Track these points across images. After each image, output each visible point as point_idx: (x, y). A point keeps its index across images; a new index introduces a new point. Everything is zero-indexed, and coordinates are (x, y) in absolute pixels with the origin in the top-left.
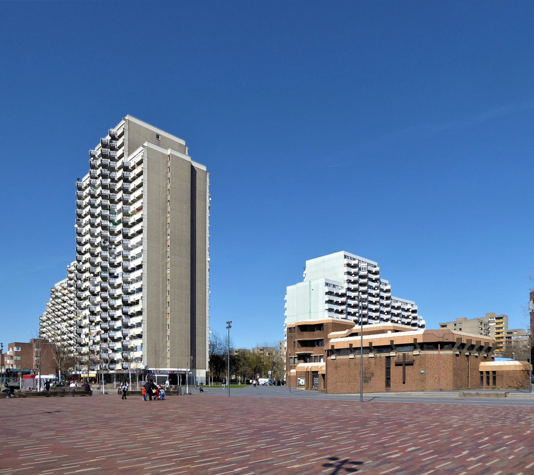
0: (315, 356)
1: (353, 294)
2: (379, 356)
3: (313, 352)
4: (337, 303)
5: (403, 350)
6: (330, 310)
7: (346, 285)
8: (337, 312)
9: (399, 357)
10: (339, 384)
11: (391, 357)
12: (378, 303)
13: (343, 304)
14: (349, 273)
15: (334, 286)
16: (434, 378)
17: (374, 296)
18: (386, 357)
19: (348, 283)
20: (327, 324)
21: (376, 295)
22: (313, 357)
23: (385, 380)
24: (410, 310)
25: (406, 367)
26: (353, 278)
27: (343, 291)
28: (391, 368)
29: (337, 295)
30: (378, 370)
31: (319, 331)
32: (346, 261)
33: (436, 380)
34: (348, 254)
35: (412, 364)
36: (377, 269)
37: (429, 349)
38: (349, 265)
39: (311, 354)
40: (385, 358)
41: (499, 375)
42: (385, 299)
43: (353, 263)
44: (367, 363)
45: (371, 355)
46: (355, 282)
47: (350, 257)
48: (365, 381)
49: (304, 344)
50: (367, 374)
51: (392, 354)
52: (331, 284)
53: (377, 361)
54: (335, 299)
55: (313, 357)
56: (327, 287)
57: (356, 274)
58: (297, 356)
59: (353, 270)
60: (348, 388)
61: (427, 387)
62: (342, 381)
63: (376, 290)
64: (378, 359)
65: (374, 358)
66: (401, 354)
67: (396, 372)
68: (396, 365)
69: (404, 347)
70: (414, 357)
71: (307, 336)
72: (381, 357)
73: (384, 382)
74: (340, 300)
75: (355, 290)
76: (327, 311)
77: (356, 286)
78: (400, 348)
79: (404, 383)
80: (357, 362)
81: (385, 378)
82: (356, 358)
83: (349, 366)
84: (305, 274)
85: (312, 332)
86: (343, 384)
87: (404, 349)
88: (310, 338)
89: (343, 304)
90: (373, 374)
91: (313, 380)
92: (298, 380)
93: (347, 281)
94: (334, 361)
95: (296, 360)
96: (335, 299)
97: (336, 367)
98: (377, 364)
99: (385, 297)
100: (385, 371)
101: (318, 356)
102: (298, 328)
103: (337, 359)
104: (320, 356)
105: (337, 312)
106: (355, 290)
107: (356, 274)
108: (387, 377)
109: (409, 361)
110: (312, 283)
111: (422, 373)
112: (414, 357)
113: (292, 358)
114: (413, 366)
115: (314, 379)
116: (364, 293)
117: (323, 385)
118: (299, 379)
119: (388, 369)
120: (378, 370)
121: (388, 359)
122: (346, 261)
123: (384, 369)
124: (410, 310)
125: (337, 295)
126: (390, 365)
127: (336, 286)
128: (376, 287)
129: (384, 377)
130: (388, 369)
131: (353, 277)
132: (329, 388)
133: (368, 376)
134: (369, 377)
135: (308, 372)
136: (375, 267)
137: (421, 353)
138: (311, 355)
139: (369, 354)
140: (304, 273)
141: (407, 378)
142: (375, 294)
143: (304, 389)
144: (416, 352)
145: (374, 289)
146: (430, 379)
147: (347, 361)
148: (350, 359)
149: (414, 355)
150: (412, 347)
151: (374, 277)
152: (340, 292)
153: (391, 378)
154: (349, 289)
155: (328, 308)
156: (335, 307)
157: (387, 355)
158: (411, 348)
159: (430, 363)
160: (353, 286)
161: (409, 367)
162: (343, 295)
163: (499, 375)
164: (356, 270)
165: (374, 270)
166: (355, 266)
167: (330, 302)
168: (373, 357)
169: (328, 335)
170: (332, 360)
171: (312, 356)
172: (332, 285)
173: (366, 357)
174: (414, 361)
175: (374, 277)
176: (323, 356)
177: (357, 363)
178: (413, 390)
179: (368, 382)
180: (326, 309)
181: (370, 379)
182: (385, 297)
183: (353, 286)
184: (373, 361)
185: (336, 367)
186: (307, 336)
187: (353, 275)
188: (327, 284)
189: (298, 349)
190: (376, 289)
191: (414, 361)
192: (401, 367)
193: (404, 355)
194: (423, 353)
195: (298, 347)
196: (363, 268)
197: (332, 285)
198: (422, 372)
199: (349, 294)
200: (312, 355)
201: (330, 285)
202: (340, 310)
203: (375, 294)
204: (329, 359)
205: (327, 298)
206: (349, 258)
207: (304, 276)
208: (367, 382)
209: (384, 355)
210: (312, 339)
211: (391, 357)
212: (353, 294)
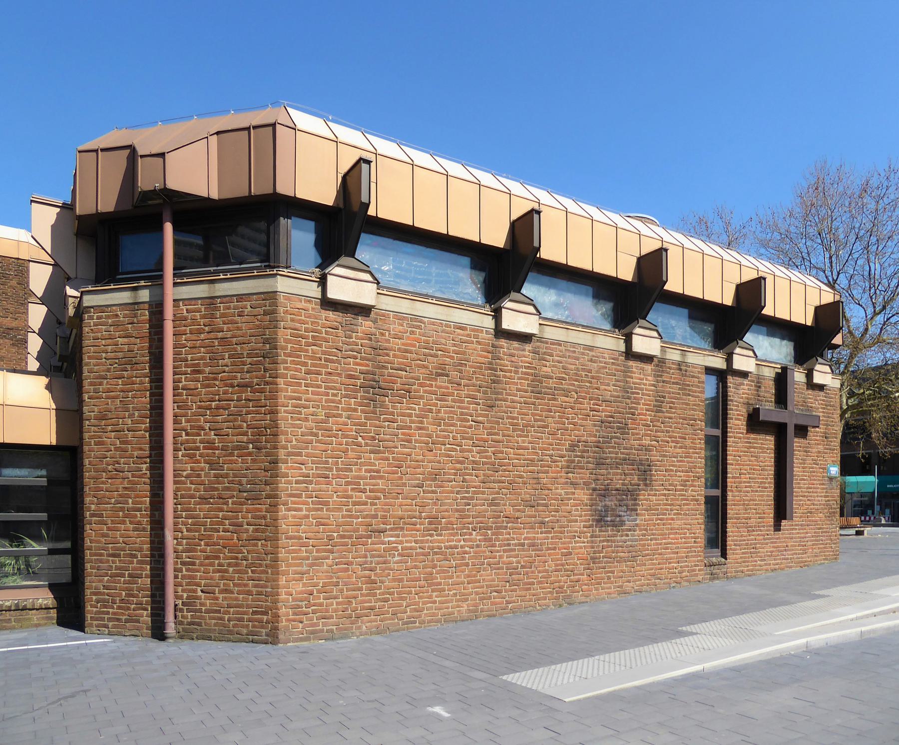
10: (407, 539)
30: (670, 449)
44: (610, 390)
60: (488, 575)
62: (434, 520)
64: (673, 375)
65: (649, 368)
82: (541, 339)
86: (441, 540)
90: (645, 472)
94: (350, 329)
98: (666, 407)
103: (385, 315)
132: (298, 588)
147: (477, 355)
170: (331, 315)
177: (551, 383)
204: (290, 296)
208: (614, 525)
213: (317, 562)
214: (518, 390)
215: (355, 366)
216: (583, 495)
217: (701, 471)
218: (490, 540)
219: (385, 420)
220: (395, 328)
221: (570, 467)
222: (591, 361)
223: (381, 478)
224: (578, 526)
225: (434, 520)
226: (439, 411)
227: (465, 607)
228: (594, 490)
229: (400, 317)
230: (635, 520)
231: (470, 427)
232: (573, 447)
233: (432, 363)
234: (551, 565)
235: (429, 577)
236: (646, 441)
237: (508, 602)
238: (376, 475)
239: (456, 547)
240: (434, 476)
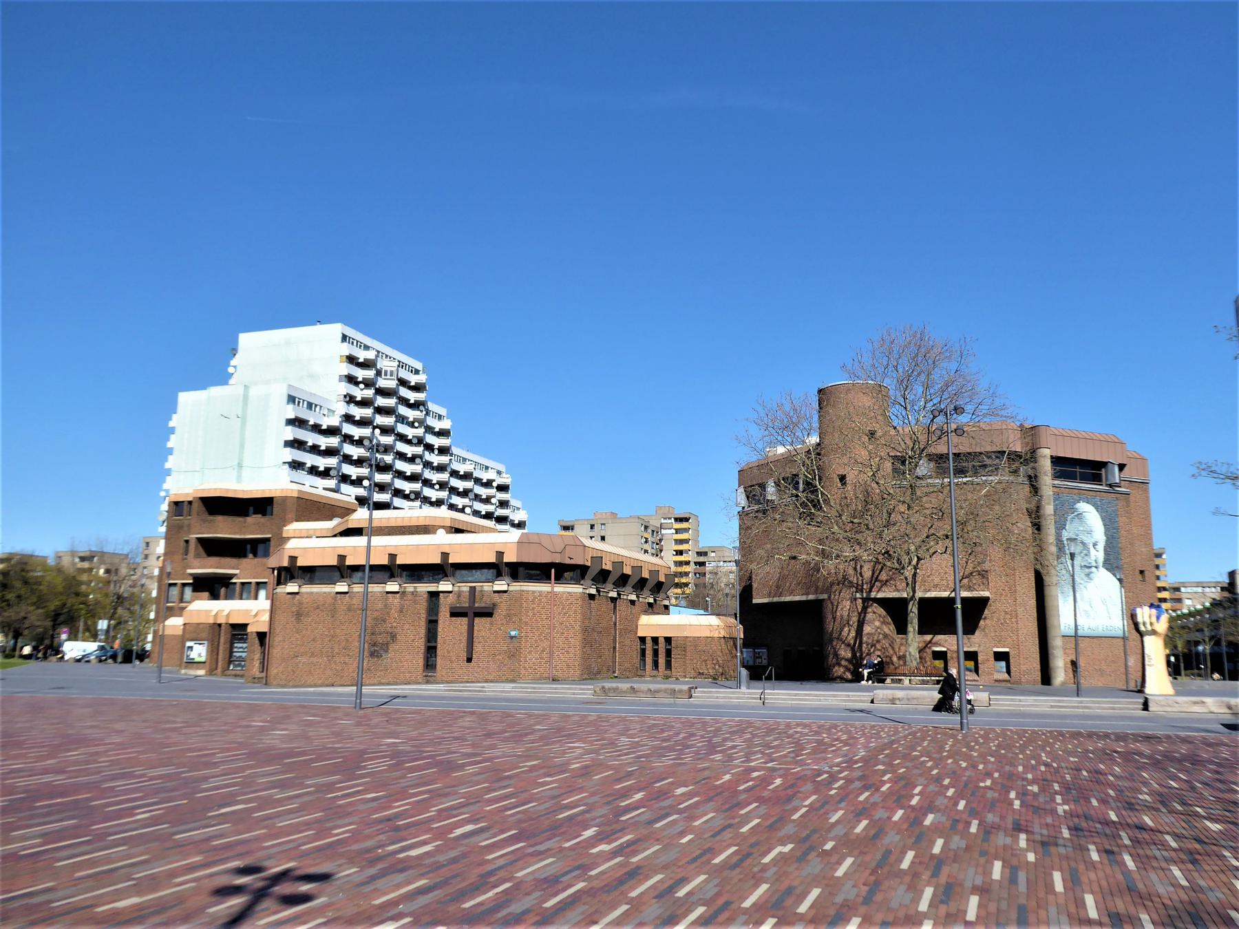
0: (243, 584)
1: (357, 432)
2: (411, 589)
3: (237, 572)
4: (315, 449)
5: (470, 579)
6: (296, 465)
7: (342, 408)
8: (313, 471)
9: (459, 594)
10: (303, 659)
11: (441, 594)
12: (418, 460)
13: (330, 452)
14: (351, 379)
15: (310, 405)
16: (540, 649)
17: (409, 442)
18: (429, 592)
19: (348, 403)
20: (285, 499)
21: (415, 441)
22: (238, 587)
23: (422, 651)
24: (495, 484)
25: (477, 620)
26: (360, 393)
27: (334, 421)
28: (440, 622)
29: (317, 428)
31: (260, 516)
32: (346, 349)
33: (544, 655)
34: (350, 332)
35: (490, 615)
36: (421, 378)
37: (531, 578)
38: (351, 360)
39: (231, 576)
40: (426, 596)
42: (436, 452)
43: (362, 355)
44: (380, 606)
45: (393, 586)
46: (364, 403)
47: (357, 341)
48: (372, 655)
49: (213, 548)
50: (380, 634)
51: (445, 586)
52: (304, 401)
53: (407, 602)
54: (312, 438)
55: (238, 587)
56: (291, 406)
57: (368, 384)
58: (191, 581)
59: (361, 374)
60: (328, 672)
61: (523, 672)
62: (313, 653)
63: (417, 428)
64: (410, 597)
65: (398, 595)
66: (465, 588)
67: (451, 631)
68: (454, 614)
69: (474, 571)
71: (225, 529)
73: (422, 656)
74: (324, 442)
75: (363, 423)
76: (287, 466)
77: (367, 412)
78: (464, 572)
79: (469, 660)
80: (354, 602)
81: (423, 647)
82: (353, 592)
83: (333, 611)
84: (235, 367)
85: (241, 519)
86: (314, 660)
87: (472, 576)
88: (234, 534)
89: (330, 452)
90: (393, 637)
91: (232, 647)
92: (189, 647)
93: (345, 396)
94: (294, 598)
95: (188, 591)
96: (312, 438)
97: (299, 615)
99: (436, 447)
100: (424, 628)
101: (250, 583)
102: (201, 504)
103: (303, 593)
104: (258, 583)
105: (313, 471)
106: (363, 423)
107: (368, 384)
109: (483, 605)
110: (253, 392)
111: (512, 637)
112: (496, 597)
113: (175, 584)
114: (493, 619)
115: (236, 645)
116: (385, 431)
117: (258, 662)
118: (189, 644)
119: (432, 624)
120: (406, 627)
121: (434, 599)
122: (346, 349)
123: (423, 623)
124: (495, 484)
125: (317, 428)
126: (437, 615)
127: (316, 405)
128: (415, 420)
129: (420, 644)
130: (432, 624)
131: (362, 390)
132: (276, 671)
133: (380, 639)
134: (382, 644)
135: (220, 625)
136: (417, 372)
137: (511, 588)
138: (231, 578)
139: (385, 584)
140: (233, 362)
141: (478, 647)
142: (413, 437)
143: (201, 672)
144: (500, 585)
145: (411, 425)
146: (530, 652)
147: (330, 600)
148: (338, 595)
149: (495, 592)
150: (491, 570)
151: (412, 396)
152: (325, 423)
153: (439, 646)
154: (348, 418)
155: (290, 460)
156: (310, 460)
157: (432, 587)
158: (490, 573)
159: (530, 613)
160: (358, 413)
161: (484, 620)
162: (332, 431)
164: (370, 374)
165: (413, 379)
166: (366, 365)
167: (297, 444)
168: (397, 593)
169: (285, 528)
171: (235, 583)
172: (305, 403)
174: (494, 605)
175: (412, 396)
176: (266, 583)
177: (355, 607)
178: (491, 677)
180: (285, 463)
181: (385, 647)
182: (436, 447)
183: (358, 413)
184: (396, 600)
185: (299, 615)
186: (225, 529)
187: (362, 386)
188: (291, 399)
189: (196, 562)
190: (416, 424)
191: (494, 605)
192: (465, 620)
193: (473, 589)
194: (517, 587)
195: (197, 556)
196: (386, 372)
197: (305, 403)
198: (513, 633)
199: (348, 429)
200: (233, 581)
201: (299, 402)
202: (322, 469)
203: (413, 437)
205: (291, 433)
206: (353, 343)
207: (231, 370)
208: (378, 657)
209: (424, 588)
210: (238, 536)
211: (441, 594)
212: (357, 432)
213: (281, 664)
215: (294, 609)
217: (423, 636)
220: (305, 596)
225: (313, 653)
227: (320, 682)
229: (307, 593)
234: (351, 670)
235: (310, 671)
236: (395, 624)
240: (313, 640)
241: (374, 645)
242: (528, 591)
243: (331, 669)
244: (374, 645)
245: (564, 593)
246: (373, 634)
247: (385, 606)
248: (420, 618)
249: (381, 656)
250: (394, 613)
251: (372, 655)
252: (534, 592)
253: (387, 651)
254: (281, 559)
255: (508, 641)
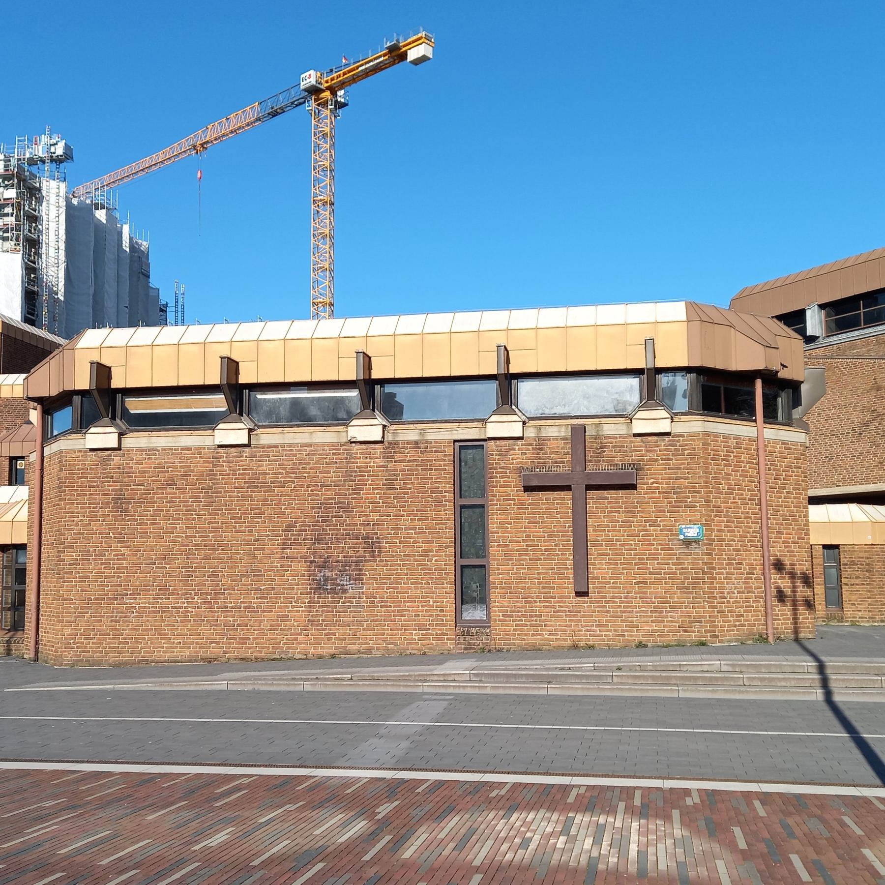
16: (745, 568)
30: (405, 522)
33: (753, 584)
41: (853, 563)
48: (319, 587)
60: (204, 629)
62: (163, 589)
70: (639, 452)
72: (427, 442)
73: (450, 588)
90: (372, 545)
100: (450, 524)
103: (129, 450)
108: (466, 562)
109: (603, 466)
111: (688, 542)
120: (405, 522)
123: (448, 512)
126: (482, 492)
133: (337, 553)
141: (599, 568)
153: (493, 564)
159: (724, 487)
163: (853, 563)
173: (332, 445)
174: (638, 468)
179: (345, 591)
191: (638, 468)
198: (692, 532)
213: (82, 615)
214: (235, 487)
216: (300, 567)
218: (210, 603)
219: (129, 520)
221: (284, 545)
222: (309, 455)
223: (124, 559)
224: (297, 591)
226: (168, 511)
228: (312, 562)
229: (140, 450)
230: (362, 588)
231: (194, 519)
232: (289, 528)
233: (162, 478)
234: (265, 625)
236: (374, 517)
237: (225, 652)
238: (121, 557)
239: (181, 607)
241: (324, 565)
242: (716, 435)
243: (214, 623)
244: (324, 565)
245: (776, 441)
246: (318, 540)
247: (348, 474)
248: (439, 503)
249: (345, 591)
250: (371, 491)
251: (319, 587)
252: (726, 437)
253: (358, 578)
254: (65, 370)
255: (678, 550)
